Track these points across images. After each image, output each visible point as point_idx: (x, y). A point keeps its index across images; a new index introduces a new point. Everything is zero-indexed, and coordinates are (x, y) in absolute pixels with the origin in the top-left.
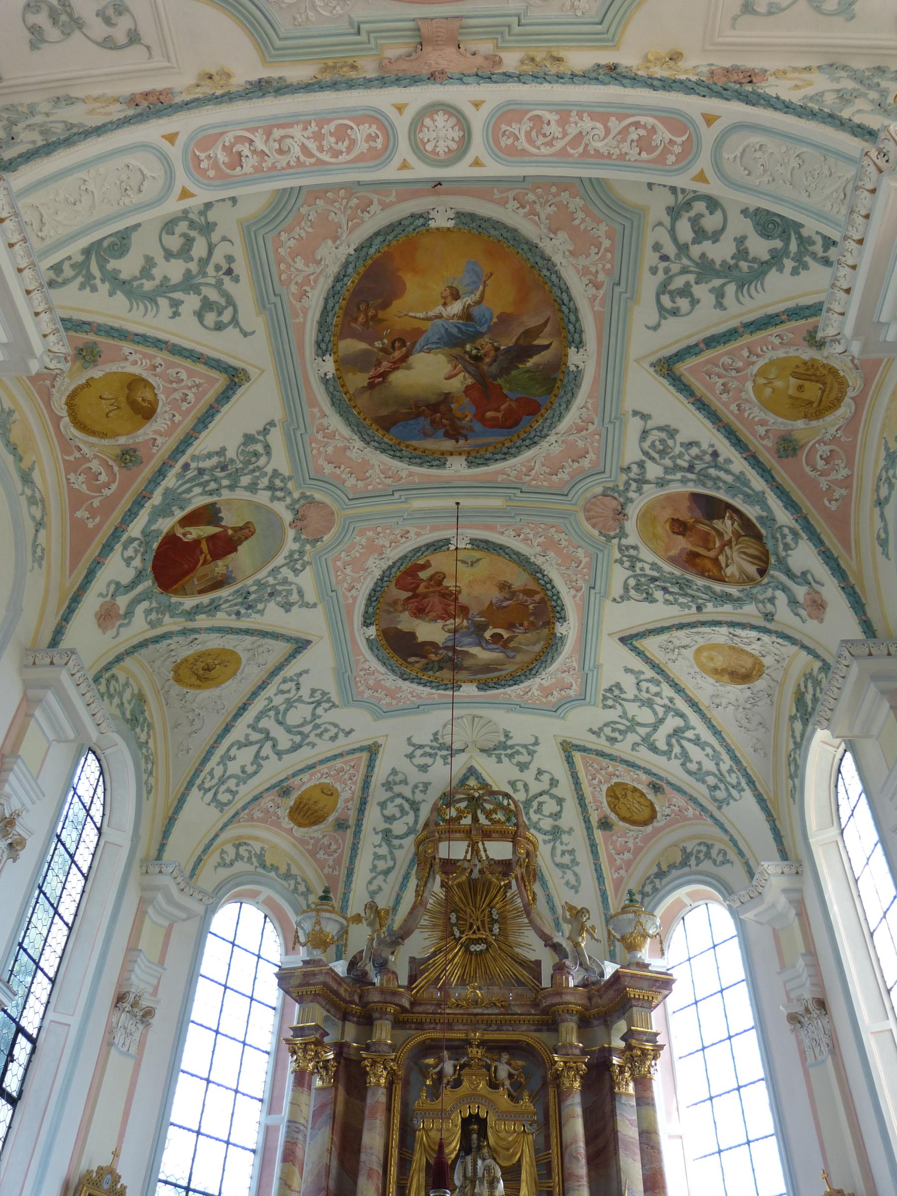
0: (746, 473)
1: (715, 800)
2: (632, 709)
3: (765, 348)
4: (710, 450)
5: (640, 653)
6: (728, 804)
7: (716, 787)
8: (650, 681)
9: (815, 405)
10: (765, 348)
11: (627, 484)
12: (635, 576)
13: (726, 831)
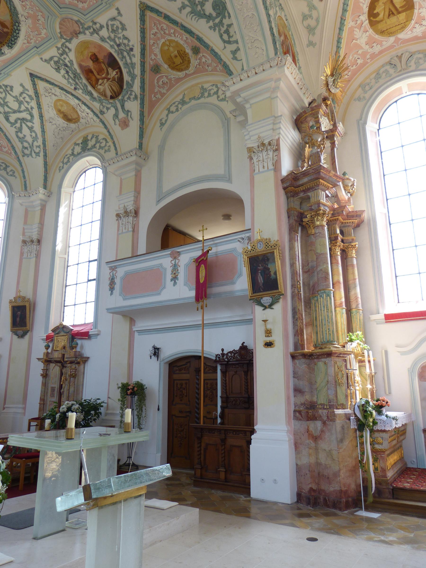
0: (137, 65)
1: (23, 152)
2: (9, 99)
3: (179, 36)
4: (131, 47)
5: (34, 85)
6: (28, 157)
7: (26, 148)
8: (30, 96)
9: (175, 65)
10: (179, 36)
11: (89, 28)
12: (59, 58)
13: (21, 166)
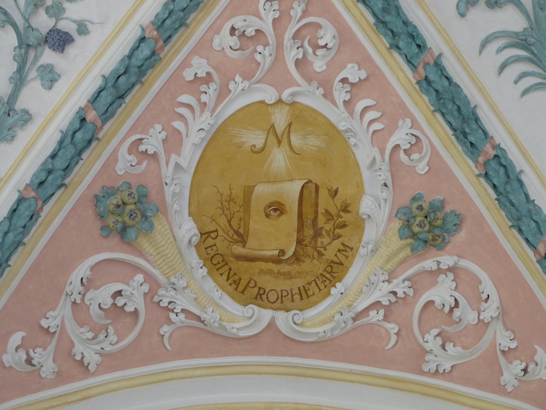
0: (32, 129)
3: (371, 115)
4: (65, 25)
9: (239, 249)
10: (371, 115)
